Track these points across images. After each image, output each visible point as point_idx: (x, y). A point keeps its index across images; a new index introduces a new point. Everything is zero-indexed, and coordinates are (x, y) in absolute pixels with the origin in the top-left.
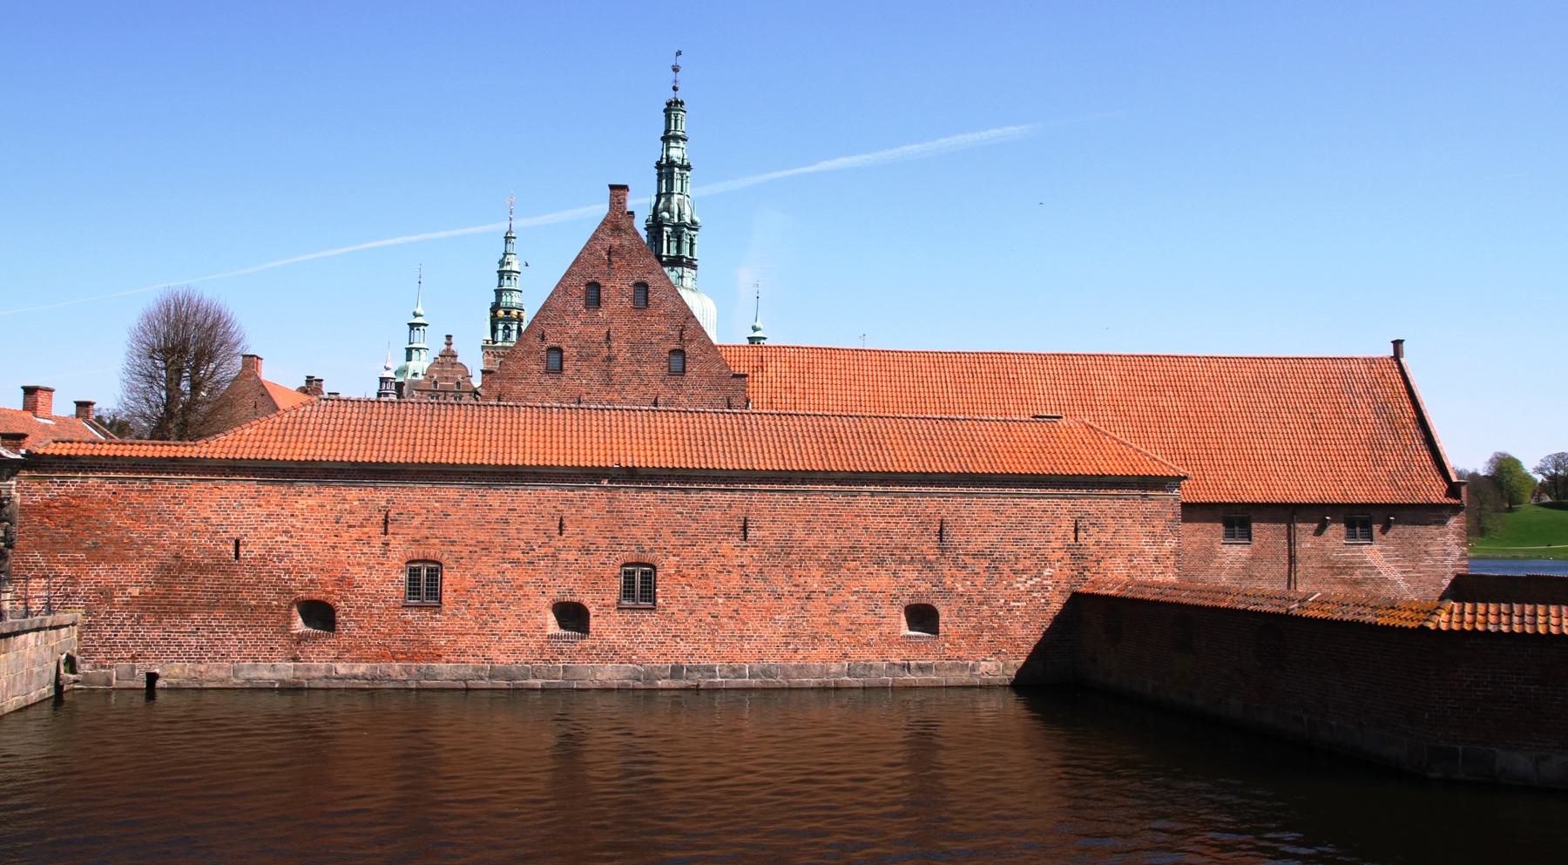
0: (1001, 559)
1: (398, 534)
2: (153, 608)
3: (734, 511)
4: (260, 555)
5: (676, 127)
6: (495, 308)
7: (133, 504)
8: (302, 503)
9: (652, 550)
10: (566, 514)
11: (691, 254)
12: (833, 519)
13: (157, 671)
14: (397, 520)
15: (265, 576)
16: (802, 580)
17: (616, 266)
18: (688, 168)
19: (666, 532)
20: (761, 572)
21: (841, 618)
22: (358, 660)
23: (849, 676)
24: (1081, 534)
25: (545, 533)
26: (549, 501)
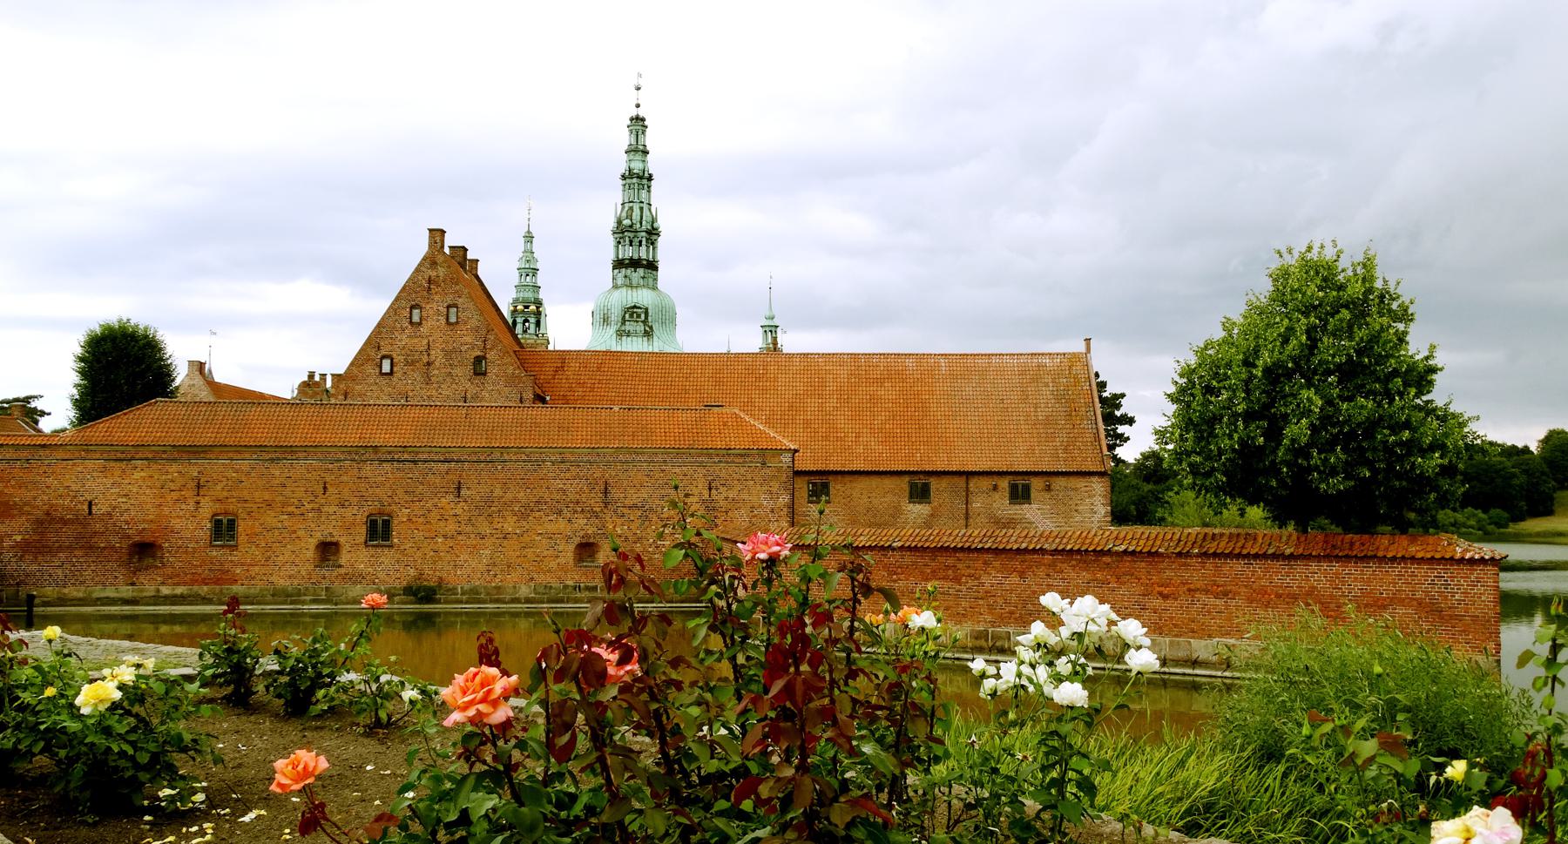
0: (651, 509)
8: (137, 475)
10: (328, 480)
17: (433, 291)
19: (400, 492)
22: (178, 584)
24: (713, 491)
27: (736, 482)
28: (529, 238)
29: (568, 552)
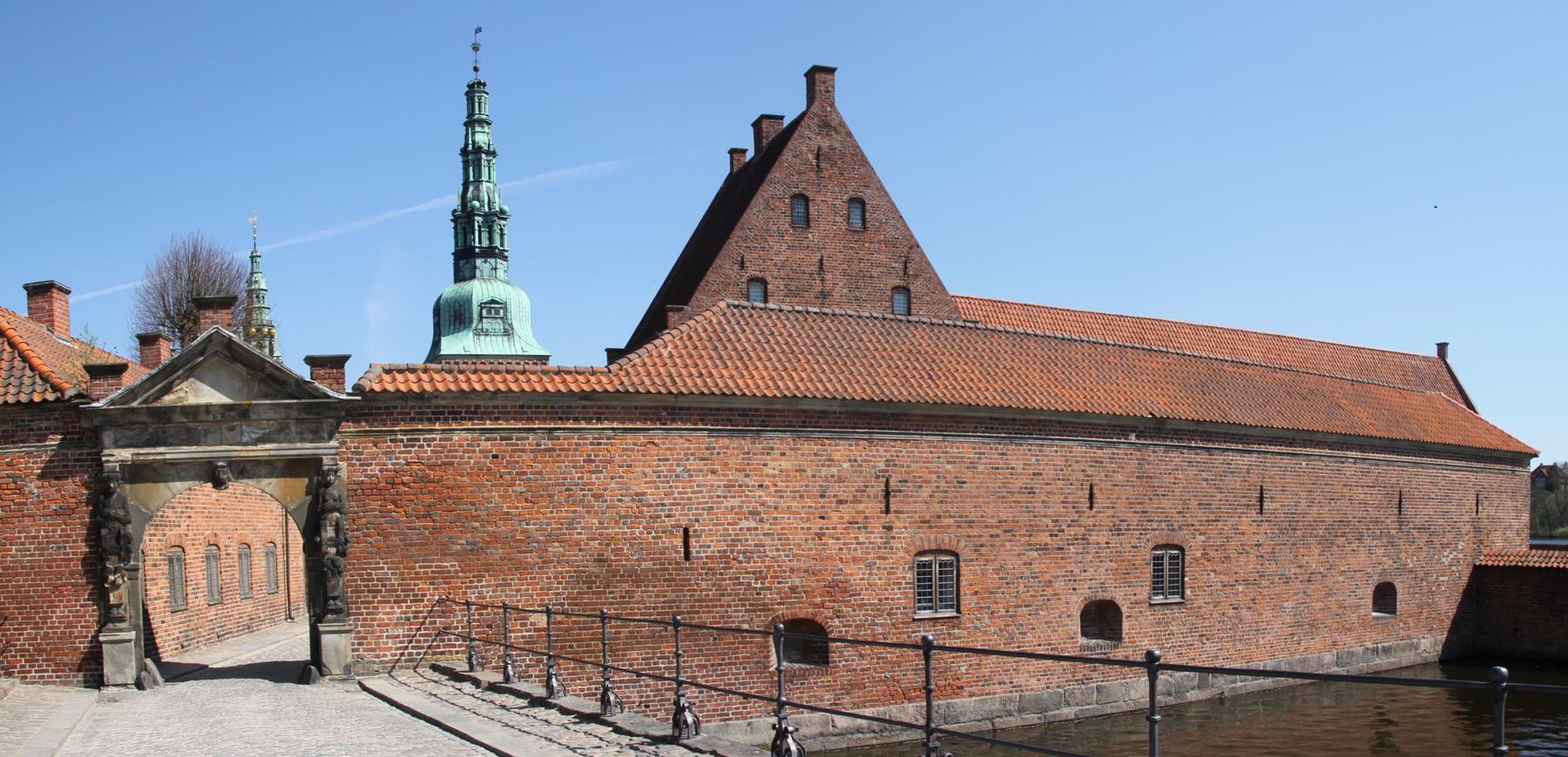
1: (902, 512)
2: (571, 647)
4: (719, 552)
7: (525, 473)
8: (774, 466)
11: (502, 245)
14: (900, 491)
15: (729, 585)
18: (493, 154)
23: (1337, 665)
25: (1074, 507)
26: (1077, 462)
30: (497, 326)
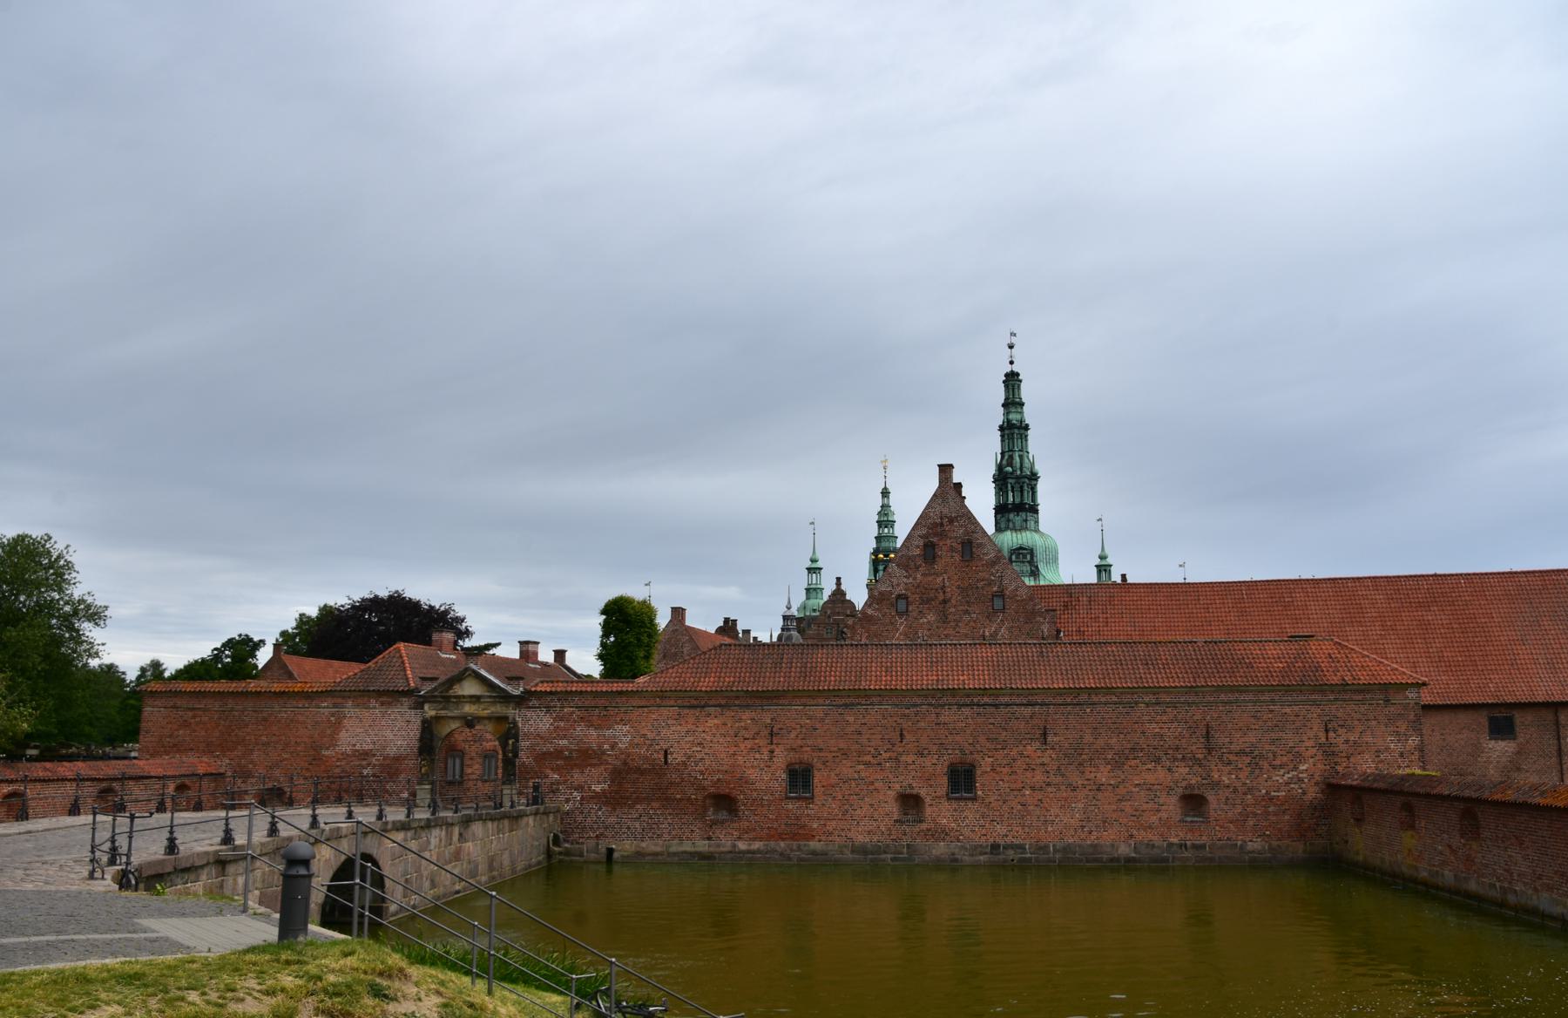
0: (1261, 756)
3: (1035, 721)
5: (1013, 395)
6: (876, 552)
8: (712, 722)
9: (971, 753)
10: (904, 726)
12: (1115, 726)
13: (614, 846)
16: (1093, 775)
19: (982, 739)
20: (1059, 769)
21: (1126, 805)
22: (754, 839)
24: (1331, 734)
27: (1356, 722)
28: (885, 493)
29: (1171, 806)
30: (1025, 569)
